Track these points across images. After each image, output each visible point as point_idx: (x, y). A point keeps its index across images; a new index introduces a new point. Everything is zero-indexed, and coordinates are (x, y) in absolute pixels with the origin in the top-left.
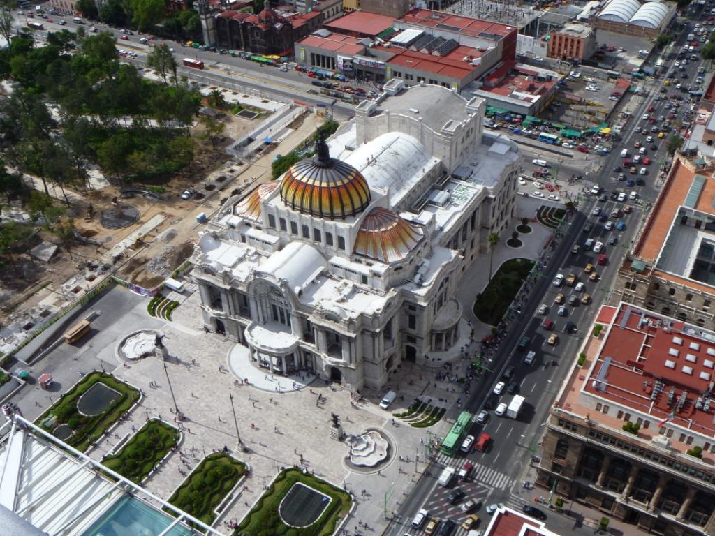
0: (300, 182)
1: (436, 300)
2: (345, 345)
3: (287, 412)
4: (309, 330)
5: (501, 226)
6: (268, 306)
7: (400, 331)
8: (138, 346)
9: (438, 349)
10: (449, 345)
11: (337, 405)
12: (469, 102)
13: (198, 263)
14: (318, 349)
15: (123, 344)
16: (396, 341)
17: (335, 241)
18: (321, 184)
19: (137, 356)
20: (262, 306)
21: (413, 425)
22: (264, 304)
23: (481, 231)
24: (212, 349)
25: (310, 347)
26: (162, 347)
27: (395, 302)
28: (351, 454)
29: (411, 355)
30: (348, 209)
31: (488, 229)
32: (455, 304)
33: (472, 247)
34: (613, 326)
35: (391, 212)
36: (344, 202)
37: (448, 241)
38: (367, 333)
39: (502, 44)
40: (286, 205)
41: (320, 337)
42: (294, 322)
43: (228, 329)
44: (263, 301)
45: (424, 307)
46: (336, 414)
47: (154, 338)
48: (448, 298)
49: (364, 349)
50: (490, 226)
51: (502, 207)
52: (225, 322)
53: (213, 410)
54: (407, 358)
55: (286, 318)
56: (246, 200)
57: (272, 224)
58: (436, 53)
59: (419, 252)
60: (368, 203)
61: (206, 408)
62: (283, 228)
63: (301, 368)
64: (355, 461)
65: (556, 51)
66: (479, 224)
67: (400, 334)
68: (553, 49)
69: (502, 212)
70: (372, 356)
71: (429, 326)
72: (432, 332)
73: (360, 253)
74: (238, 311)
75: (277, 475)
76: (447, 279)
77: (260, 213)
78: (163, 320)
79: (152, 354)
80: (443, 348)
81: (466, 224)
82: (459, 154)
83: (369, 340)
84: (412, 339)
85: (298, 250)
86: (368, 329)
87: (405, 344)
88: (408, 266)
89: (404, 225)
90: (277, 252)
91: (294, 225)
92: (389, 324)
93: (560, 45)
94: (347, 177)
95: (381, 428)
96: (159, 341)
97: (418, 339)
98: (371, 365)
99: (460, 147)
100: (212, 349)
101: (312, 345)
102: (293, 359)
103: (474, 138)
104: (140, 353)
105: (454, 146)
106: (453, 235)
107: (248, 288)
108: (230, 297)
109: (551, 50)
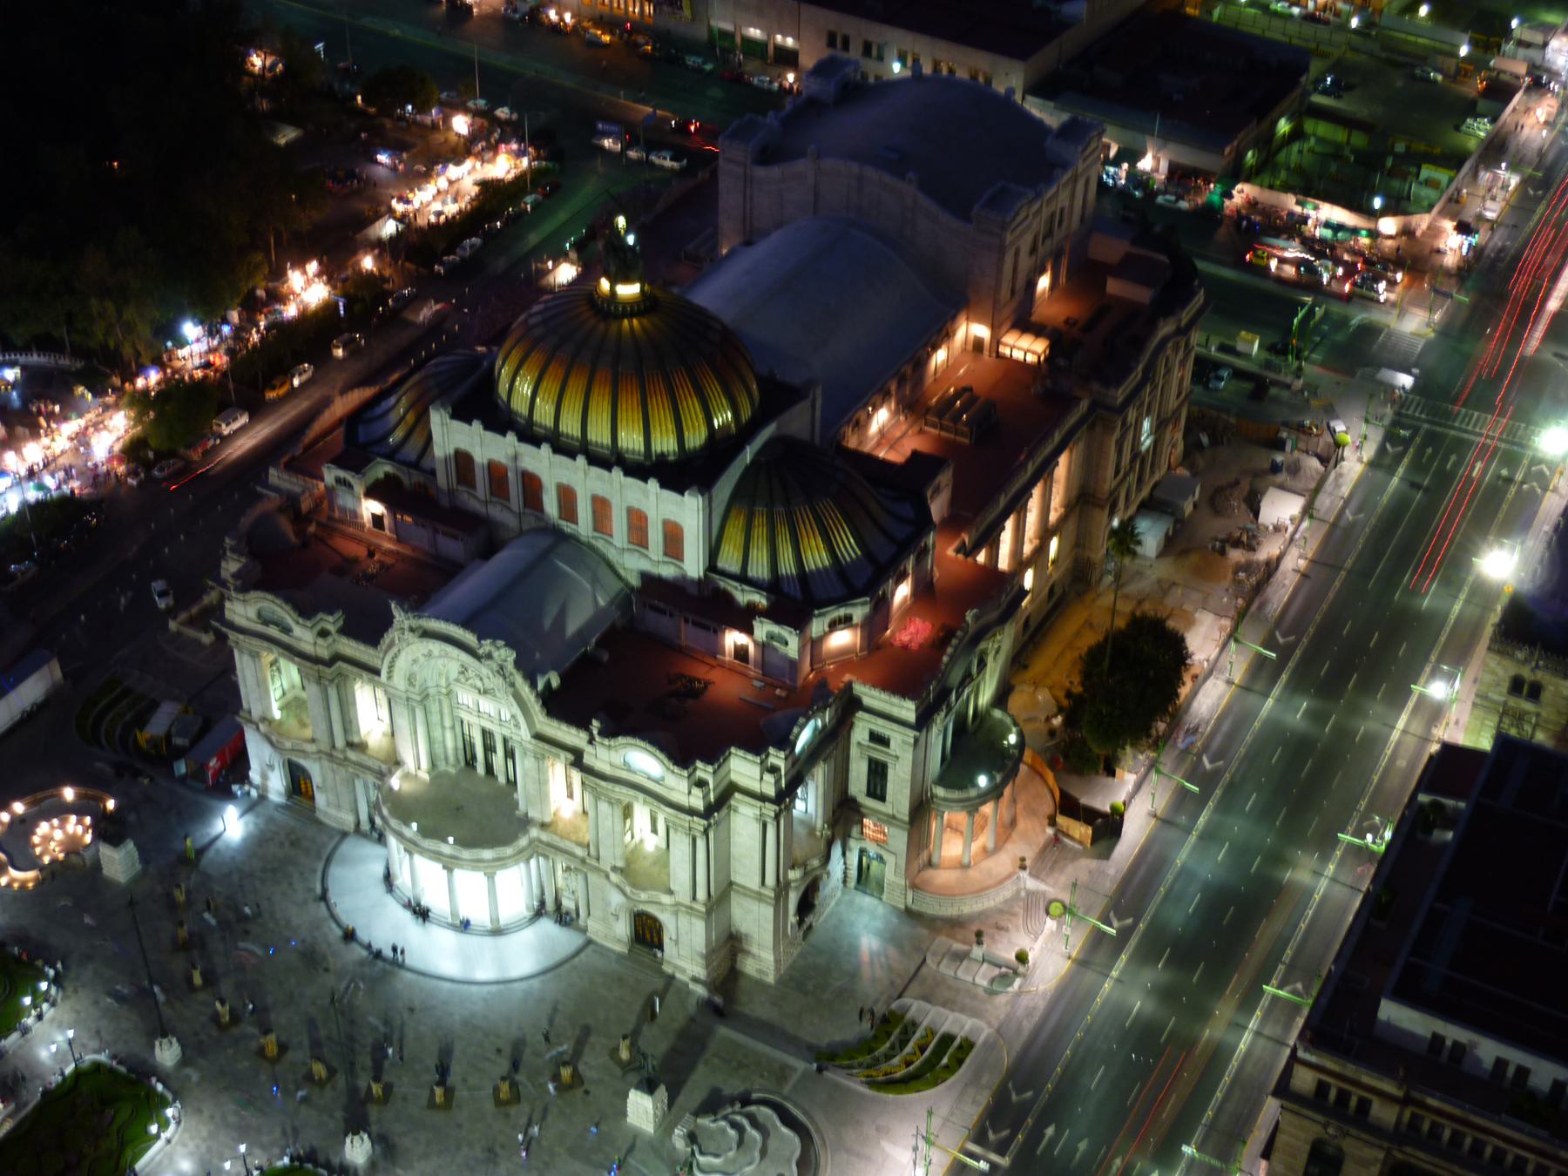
6: (448, 723)
17: (655, 536)
22: (435, 718)
44: (434, 707)
70: (757, 879)
108: (332, 692)
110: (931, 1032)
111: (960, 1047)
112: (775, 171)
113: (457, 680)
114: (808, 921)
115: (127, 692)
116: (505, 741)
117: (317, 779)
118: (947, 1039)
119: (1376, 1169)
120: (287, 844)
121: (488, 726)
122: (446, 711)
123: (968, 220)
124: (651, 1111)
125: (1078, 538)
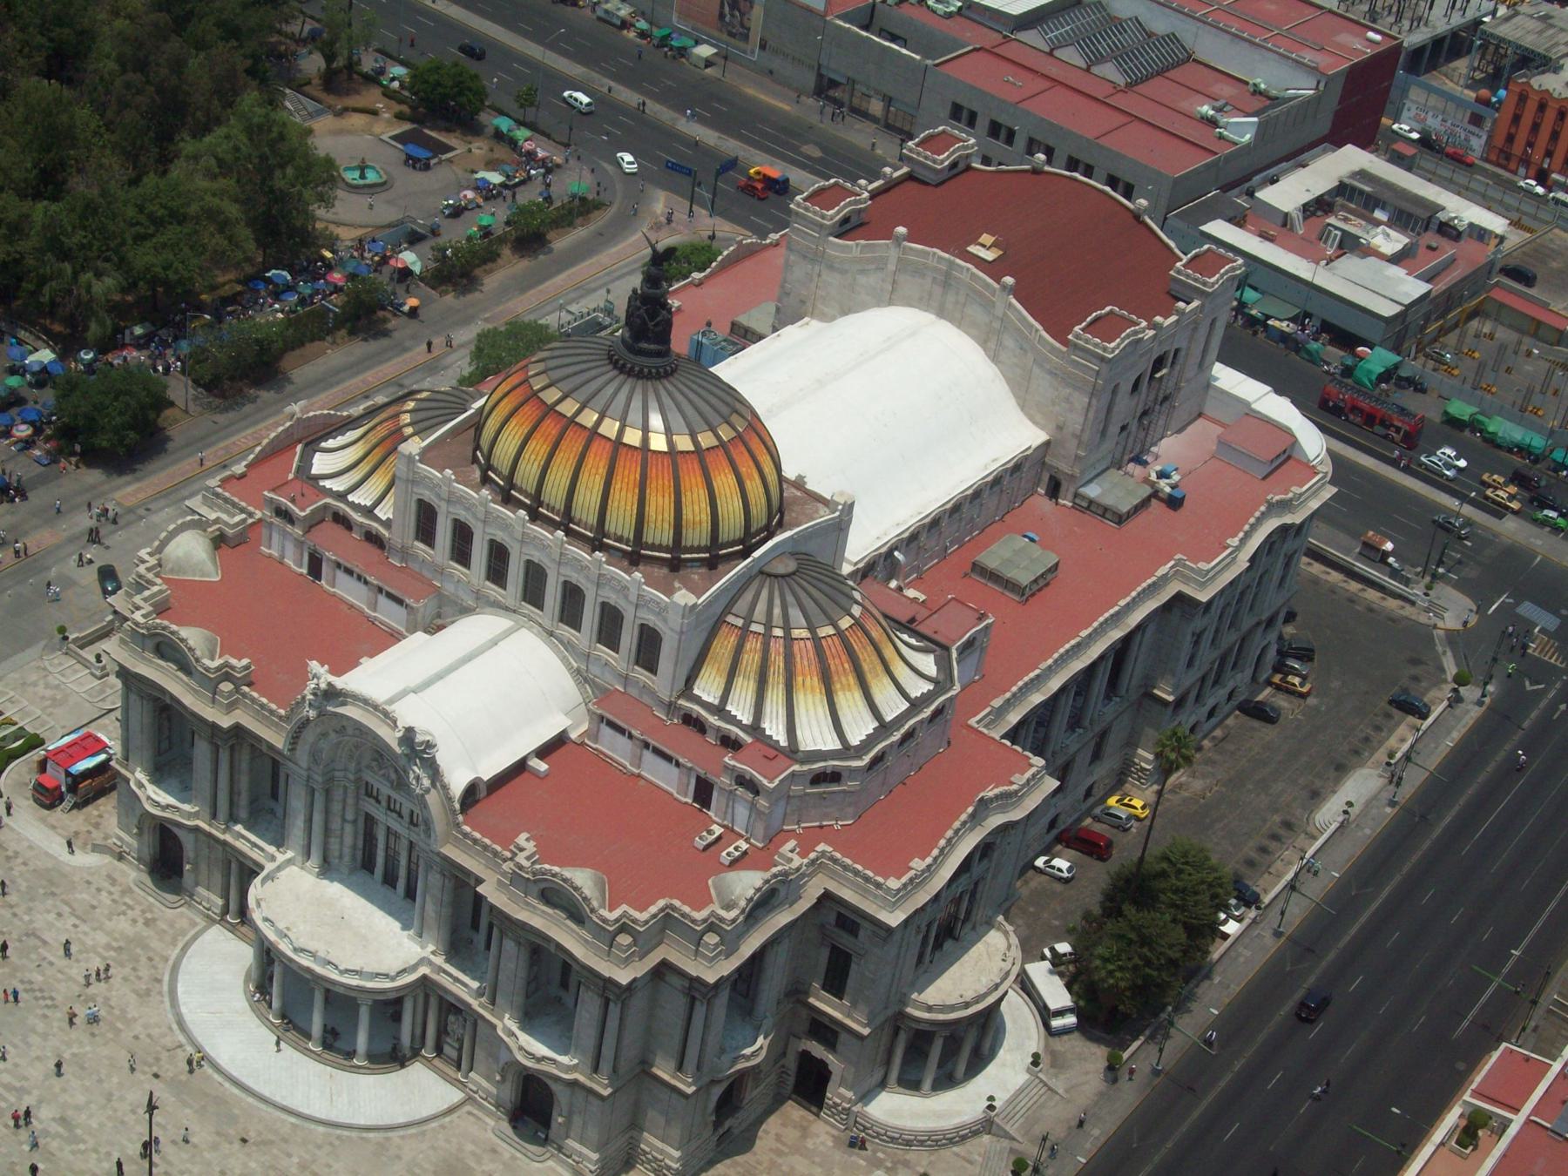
0: (550, 410)
2: (588, 1009)
4: (475, 926)
5: (1211, 702)
6: (350, 816)
7: (788, 994)
12: (1185, 259)
13: (138, 616)
17: (629, 638)
20: (327, 812)
22: (336, 807)
24: (123, 924)
25: (463, 986)
30: (697, 533)
33: (1097, 756)
34: (1528, 1122)
36: (687, 513)
39: (1338, 89)
40: (485, 480)
41: (512, 961)
44: (338, 794)
45: (889, 930)
51: (1230, 638)
52: (187, 841)
53: (77, 1140)
55: (402, 873)
56: (351, 435)
57: (426, 532)
58: (1109, 71)
61: (55, 1128)
62: (461, 554)
65: (1517, 149)
66: (1135, 682)
68: (1510, 138)
69: (1223, 659)
73: (705, 697)
74: (243, 814)
82: (1114, 429)
83: (673, 1004)
84: (826, 1031)
85: (494, 642)
89: (876, 633)
93: (1535, 127)
94: (713, 430)
97: (843, 1036)
100: (123, 924)
102: (397, 1017)
105: (1106, 397)
107: (295, 738)
108: (224, 756)
109: (1499, 141)
112: (854, 247)
113: (368, 767)
114: (727, 1125)
116: (411, 845)
120: (141, 921)
123: (1065, 343)
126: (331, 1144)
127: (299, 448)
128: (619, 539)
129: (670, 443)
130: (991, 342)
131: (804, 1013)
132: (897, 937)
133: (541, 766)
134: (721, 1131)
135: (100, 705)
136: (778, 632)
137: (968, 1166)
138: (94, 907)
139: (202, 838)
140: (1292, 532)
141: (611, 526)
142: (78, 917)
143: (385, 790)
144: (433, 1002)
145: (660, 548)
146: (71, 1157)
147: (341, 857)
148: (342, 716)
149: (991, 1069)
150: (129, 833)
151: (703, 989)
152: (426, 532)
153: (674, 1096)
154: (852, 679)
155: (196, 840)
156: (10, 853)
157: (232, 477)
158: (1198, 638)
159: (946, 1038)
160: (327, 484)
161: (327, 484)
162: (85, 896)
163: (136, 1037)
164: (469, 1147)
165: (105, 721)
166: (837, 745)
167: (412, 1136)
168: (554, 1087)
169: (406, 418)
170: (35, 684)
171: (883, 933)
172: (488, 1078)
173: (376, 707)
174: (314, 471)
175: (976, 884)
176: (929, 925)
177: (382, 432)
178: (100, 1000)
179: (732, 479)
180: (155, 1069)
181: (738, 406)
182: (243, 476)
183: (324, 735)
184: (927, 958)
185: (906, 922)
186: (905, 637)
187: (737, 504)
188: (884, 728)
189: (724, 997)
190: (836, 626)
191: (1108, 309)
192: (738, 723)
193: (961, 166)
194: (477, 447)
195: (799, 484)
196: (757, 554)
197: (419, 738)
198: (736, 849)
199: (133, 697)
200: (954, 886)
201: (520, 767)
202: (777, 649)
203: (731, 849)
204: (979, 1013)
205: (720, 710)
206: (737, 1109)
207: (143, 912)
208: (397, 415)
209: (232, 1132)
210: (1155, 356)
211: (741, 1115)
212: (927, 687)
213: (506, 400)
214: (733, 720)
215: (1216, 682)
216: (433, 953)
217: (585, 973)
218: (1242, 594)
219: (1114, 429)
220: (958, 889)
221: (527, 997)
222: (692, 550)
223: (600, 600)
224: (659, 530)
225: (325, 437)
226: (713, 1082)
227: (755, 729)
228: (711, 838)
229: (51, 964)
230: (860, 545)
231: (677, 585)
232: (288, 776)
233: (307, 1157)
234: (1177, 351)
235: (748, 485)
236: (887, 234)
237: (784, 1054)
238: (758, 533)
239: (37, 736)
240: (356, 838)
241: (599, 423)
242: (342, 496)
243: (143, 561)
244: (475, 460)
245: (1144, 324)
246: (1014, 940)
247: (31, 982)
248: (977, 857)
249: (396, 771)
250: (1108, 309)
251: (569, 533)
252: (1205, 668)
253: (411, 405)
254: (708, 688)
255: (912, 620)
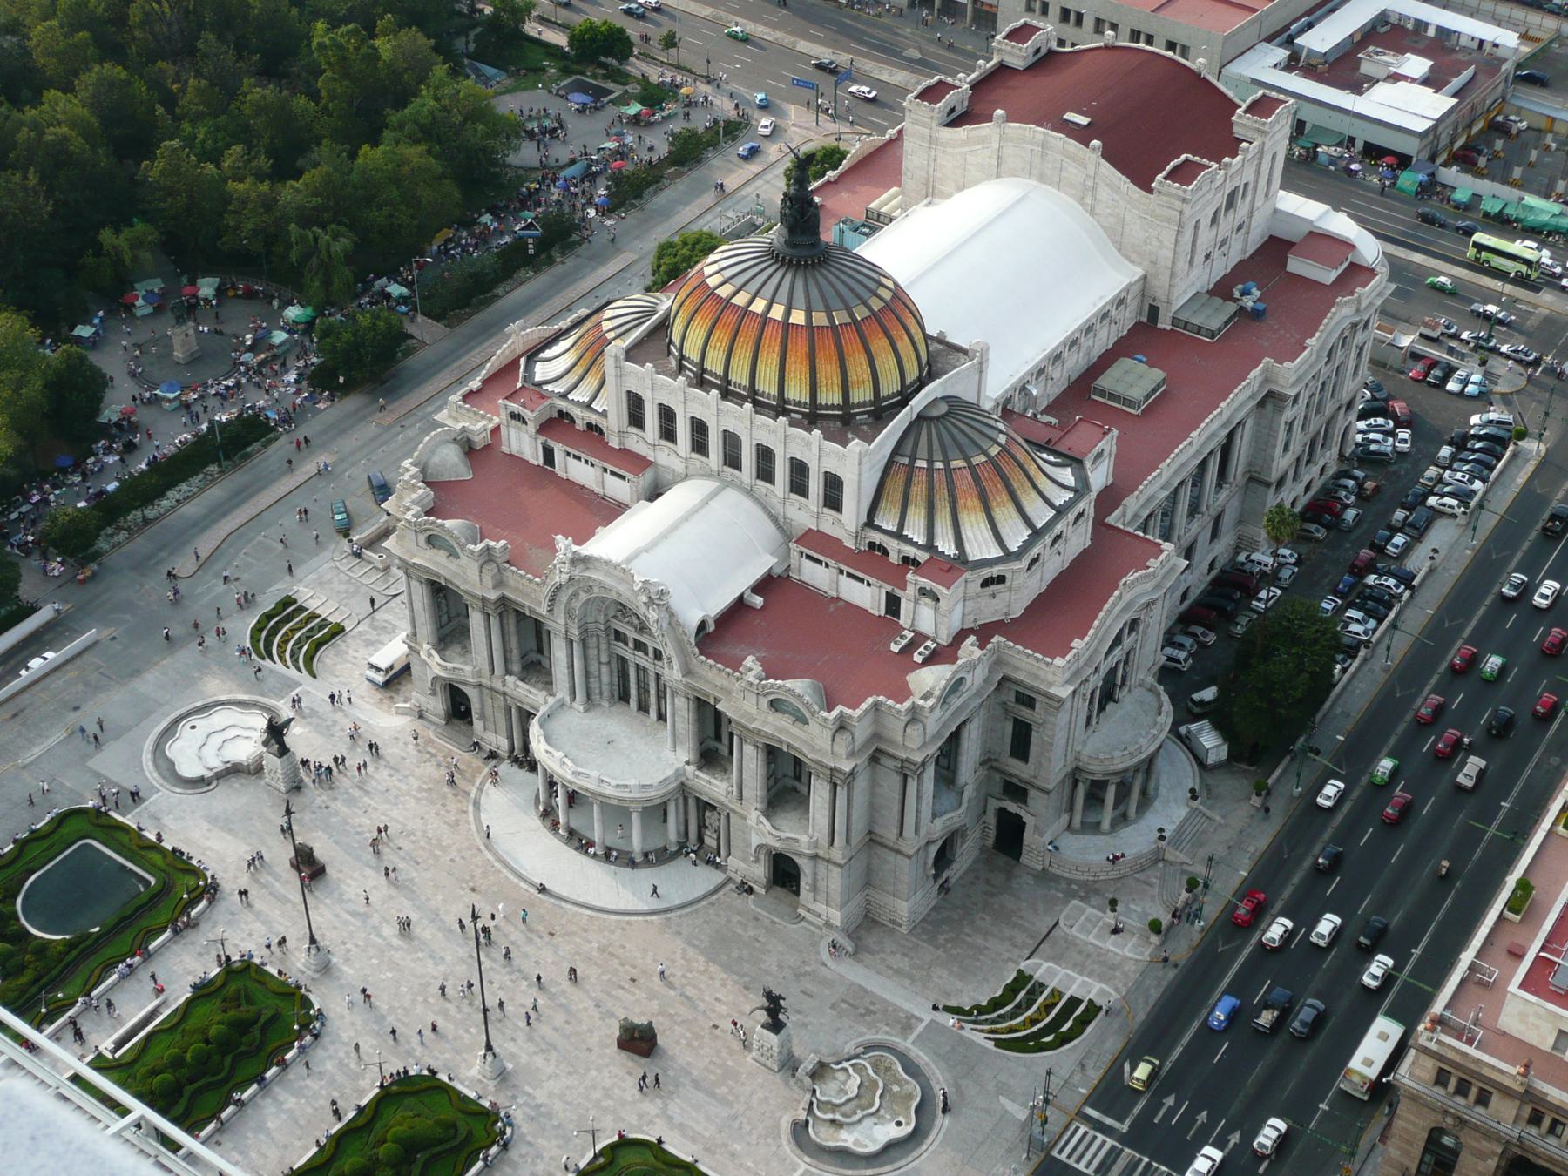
0: (726, 303)
1: (1096, 681)
2: (819, 794)
3: (634, 973)
4: (718, 738)
5: (1306, 480)
6: (604, 659)
7: (982, 764)
8: (216, 740)
9: (1095, 828)
10: (1122, 819)
11: (780, 967)
12: (1244, 107)
13: (409, 516)
14: (741, 797)
15: (169, 732)
16: (969, 793)
17: (815, 485)
18: (788, 314)
19: (208, 774)
20: (585, 658)
21: (999, 1043)
22: (592, 653)
23: (1247, 486)
25: (714, 787)
26: (283, 751)
27: (975, 679)
28: (810, 1110)
29: (1010, 835)
30: (861, 394)
31: (1268, 485)
32: (1150, 698)
33: (1215, 535)
35: (986, 414)
36: (852, 376)
37: (1145, 514)
38: (884, 760)
41: (750, 762)
42: (681, 711)
43: (483, 717)
44: (592, 642)
45: (1061, 701)
46: (776, 992)
47: (261, 722)
48: (1132, 681)
49: (873, 809)
50: (1274, 476)
51: (1316, 423)
52: (472, 694)
54: (995, 847)
55: (653, 699)
56: (564, 344)
57: (637, 420)
59: (1058, 537)
60: (921, 383)
62: (668, 434)
63: (682, 850)
64: (823, 1136)
67: (982, 773)
70: (896, 831)
71: (1070, 758)
72: (1075, 776)
73: (885, 526)
74: (516, 668)
75: (591, 1155)
76: (1134, 625)
77: (603, 382)
78: (293, 672)
79: (254, 770)
80: (1106, 825)
81: (1203, 465)
82: (1199, 258)
84: (1017, 791)
86: (891, 750)
87: (994, 804)
88: (1023, 576)
89: (1021, 456)
90: (643, 502)
91: (699, 428)
92: (955, 737)
94: (865, 303)
95: (907, 1044)
96: (276, 732)
97: (1032, 792)
98: (891, 857)
99: (1206, 237)
101: (724, 785)
103: (1251, 213)
104: (217, 764)
106: (1165, 493)
108: (494, 622)
110: (1057, 994)
111: (1087, 1009)
112: (962, 132)
113: (615, 617)
114: (944, 876)
115: (301, 609)
117: (475, 706)
118: (1074, 1002)
119: (1492, 1163)
121: (642, 663)
122: (603, 646)
123: (1150, 191)
124: (776, 1049)
125: (1241, 515)
126: (623, 929)
127: (522, 361)
128: (798, 404)
129: (831, 319)
130: (1087, 196)
131: (998, 777)
132: (1068, 705)
133: (758, 601)
134: (940, 881)
135: (386, 592)
136: (939, 465)
137: (1147, 888)
138: (404, 758)
139: (485, 691)
140: (1361, 326)
141: (790, 394)
142: (391, 768)
143: (631, 634)
144: (692, 803)
145: (833, 407)
146: (413, 965)
147: (601, 693)
148: (589, 579)
149: (1157, 804)
150: (423, 694)
151: (912, 767)
152: (637, 420)
153: (899, 857)
154: (1005, 497)
155: (481, 694)
156: (330, 723)
157: (471, 392)
158: (1291, 424)
159: (1118, 785)
160: (550, 387)
161: (550, 387)
162: (396, 750)
163: (452, 860)
164: (736, 918)
165: (393, 604)
166: (996, 552)
167: (687, 915)
168: (799, 861)
169: (606, 326)
170: (330, 581)
171: (1057, 705)
172: (744, 860)
173: (616, 567)
174: (538, 378)
175: (1128, 654)
176: (1093, 693)
177: (589, 339)
178: (419, 833)
179: (885, 342)
180: (471, 884)
181: (883, 280)
182: (479, 391)
183: (575, 594)
184: (1094, 721)
185: (1074, 692)
186: (1045, 456)
187: (893, 362)
188: (1037, 534)
189: (930, 772)
190: (985, 453)
191: (1183, 157)
192: (915, 544)
193: (1043, 51)
194: (671, 342)
195: (940, 340)
196: (912, 403)
197: (653, 590)
198: (926, 648)
199: (414, 583)
200: (1110, 658)
201: (740, 604)
202: (939, 478)
203: (922, 649)
204: (1143, 761)
205: (899, 535)
206: (951, 862)
207: (445, 757)
208: (599, 324)
209: (541, 928)
210: (1227, 192)
211: (955, 866)
212: (1069, 495)
213: (689, 300)
214: (910, 542)
215: (1308, 462)
216: (688, 763)
217: (814, 765)
218: (1324, 384)
219: (1199, 258)
220: (1112, 660)
221: (769, 790)
222: (859, 405)
223: (789, 456)
224: (830, 396)
225: (542, 349)
226: (929, 842)
227: (930, 546)
228: (904, 642)
229: (375, 809)
230: (997, 384)
231: (850, 436)
232: (549, 632)
233: (605, 941)
234: (1246, 184)
235: (899, 346)
236: (989, 119)
237: (985, 812)
238: (912, 384)
239: (337, 624)
240: (611, 676)
241: (769, 308)
242: (564, 396)
243: (407, 470)
244: (669, 353)
245: (1215, 166)
246: (1165, 698)
247: (361, 826)
248: (1127, 630)
249: (638, 618)
250: (1183, 157)
251: (756, 403)
252: (1299, 449)
253: (608, 313)
254: (888, 521)
255: (1049, 441)
